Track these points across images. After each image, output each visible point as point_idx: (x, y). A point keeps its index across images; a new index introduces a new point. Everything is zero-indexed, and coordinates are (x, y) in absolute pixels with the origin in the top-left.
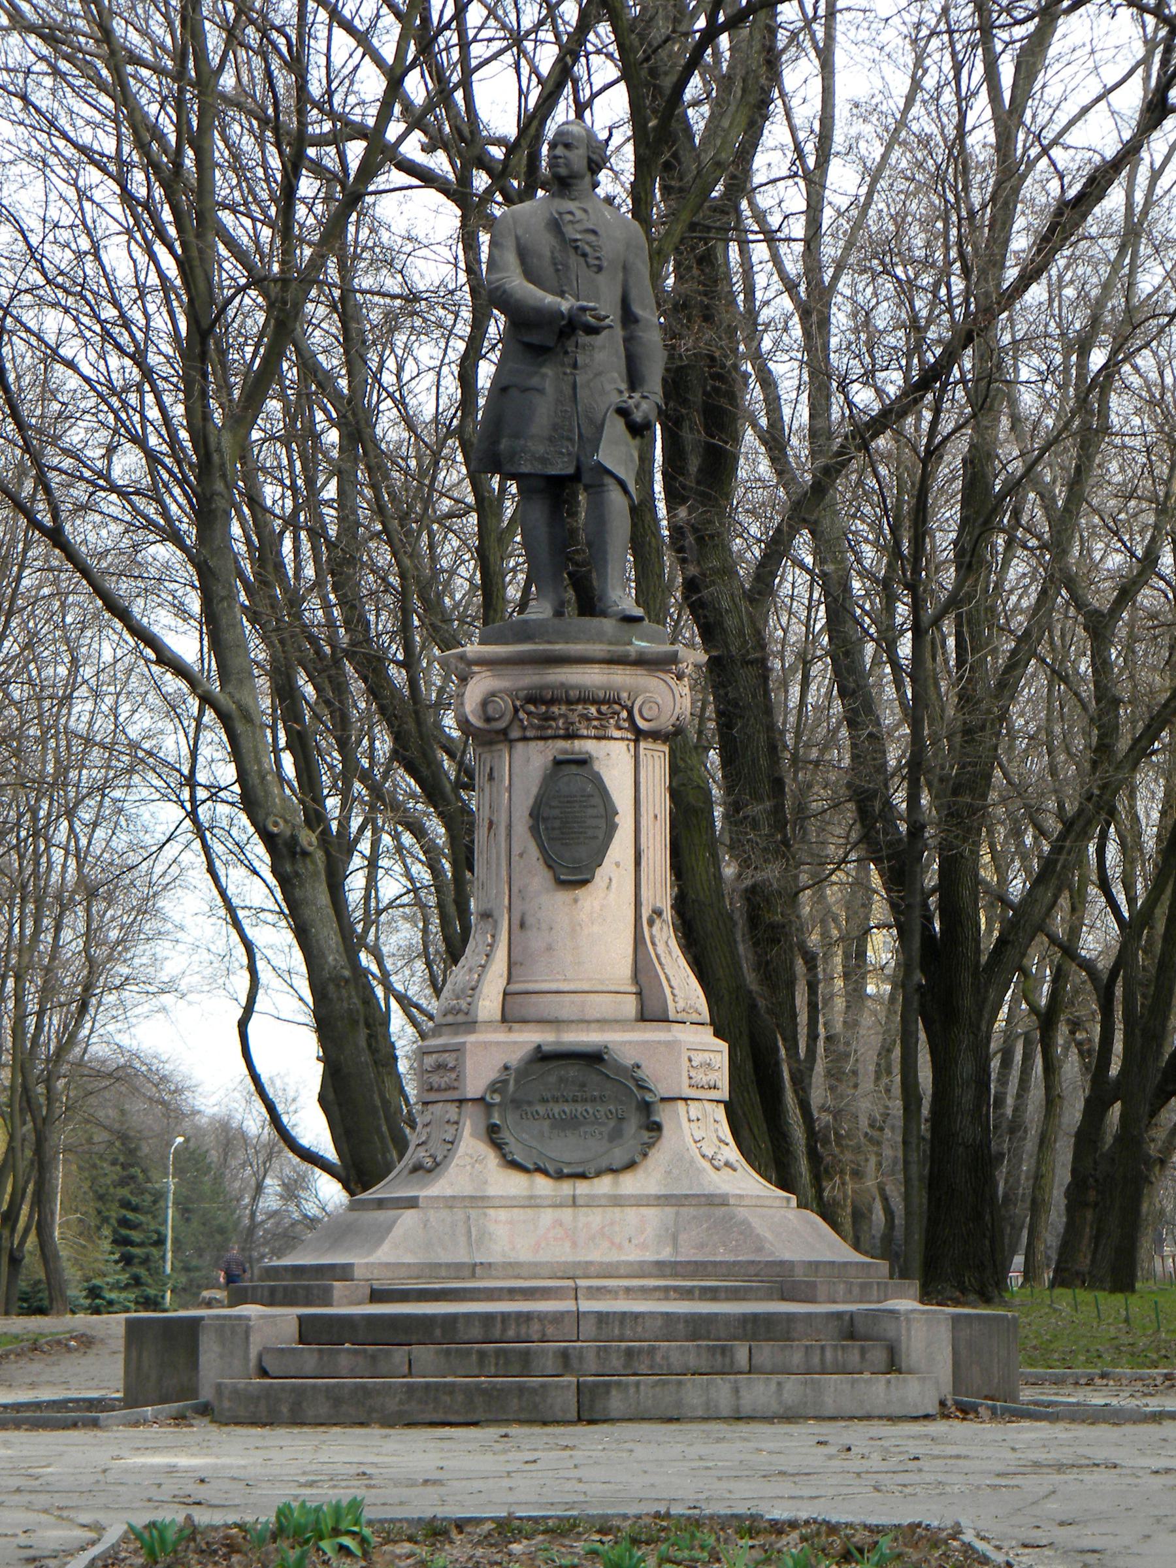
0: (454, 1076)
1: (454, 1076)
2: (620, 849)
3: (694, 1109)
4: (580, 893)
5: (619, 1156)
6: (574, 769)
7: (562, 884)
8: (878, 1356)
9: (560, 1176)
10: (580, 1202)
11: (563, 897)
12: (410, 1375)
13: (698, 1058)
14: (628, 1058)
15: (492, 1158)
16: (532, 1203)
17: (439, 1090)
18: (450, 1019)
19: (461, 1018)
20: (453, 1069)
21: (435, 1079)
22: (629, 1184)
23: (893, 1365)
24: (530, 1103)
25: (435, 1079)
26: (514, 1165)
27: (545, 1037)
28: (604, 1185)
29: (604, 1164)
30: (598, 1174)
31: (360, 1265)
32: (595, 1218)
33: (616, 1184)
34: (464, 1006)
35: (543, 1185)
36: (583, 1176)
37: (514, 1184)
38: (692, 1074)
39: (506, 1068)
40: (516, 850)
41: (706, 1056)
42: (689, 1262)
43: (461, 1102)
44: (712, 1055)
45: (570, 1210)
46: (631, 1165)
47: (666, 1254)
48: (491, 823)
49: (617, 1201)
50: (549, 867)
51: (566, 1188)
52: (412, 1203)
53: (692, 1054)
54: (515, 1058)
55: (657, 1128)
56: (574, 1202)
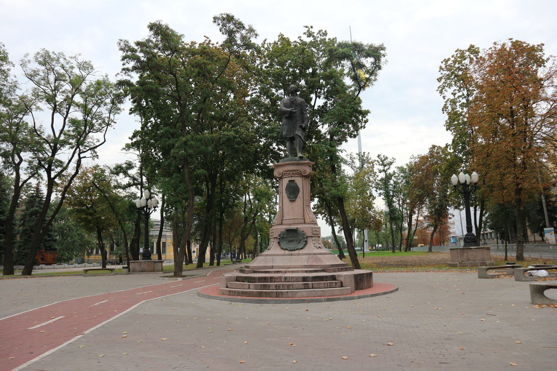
2: (300, 195)
5: (300, 247)
8: (340, 284)
9: (291, 250)
12: (249, 289)
13: (314, 229)
14: (302, 230)
15: (279, 248)
16: (284, 255)
22: (301, 252)
23: (342, 286)
26: (282, 248)
27: (288, 227)
28: (297, 252)
32: (294, 257)
35: (287, 252)
37: (283, 252)
46: (302, 248)
47: (306, 264)
49: (299, 254)
51: (291, 252)
54: (283, 230)
55: (306, 242)
56: (292, 255)
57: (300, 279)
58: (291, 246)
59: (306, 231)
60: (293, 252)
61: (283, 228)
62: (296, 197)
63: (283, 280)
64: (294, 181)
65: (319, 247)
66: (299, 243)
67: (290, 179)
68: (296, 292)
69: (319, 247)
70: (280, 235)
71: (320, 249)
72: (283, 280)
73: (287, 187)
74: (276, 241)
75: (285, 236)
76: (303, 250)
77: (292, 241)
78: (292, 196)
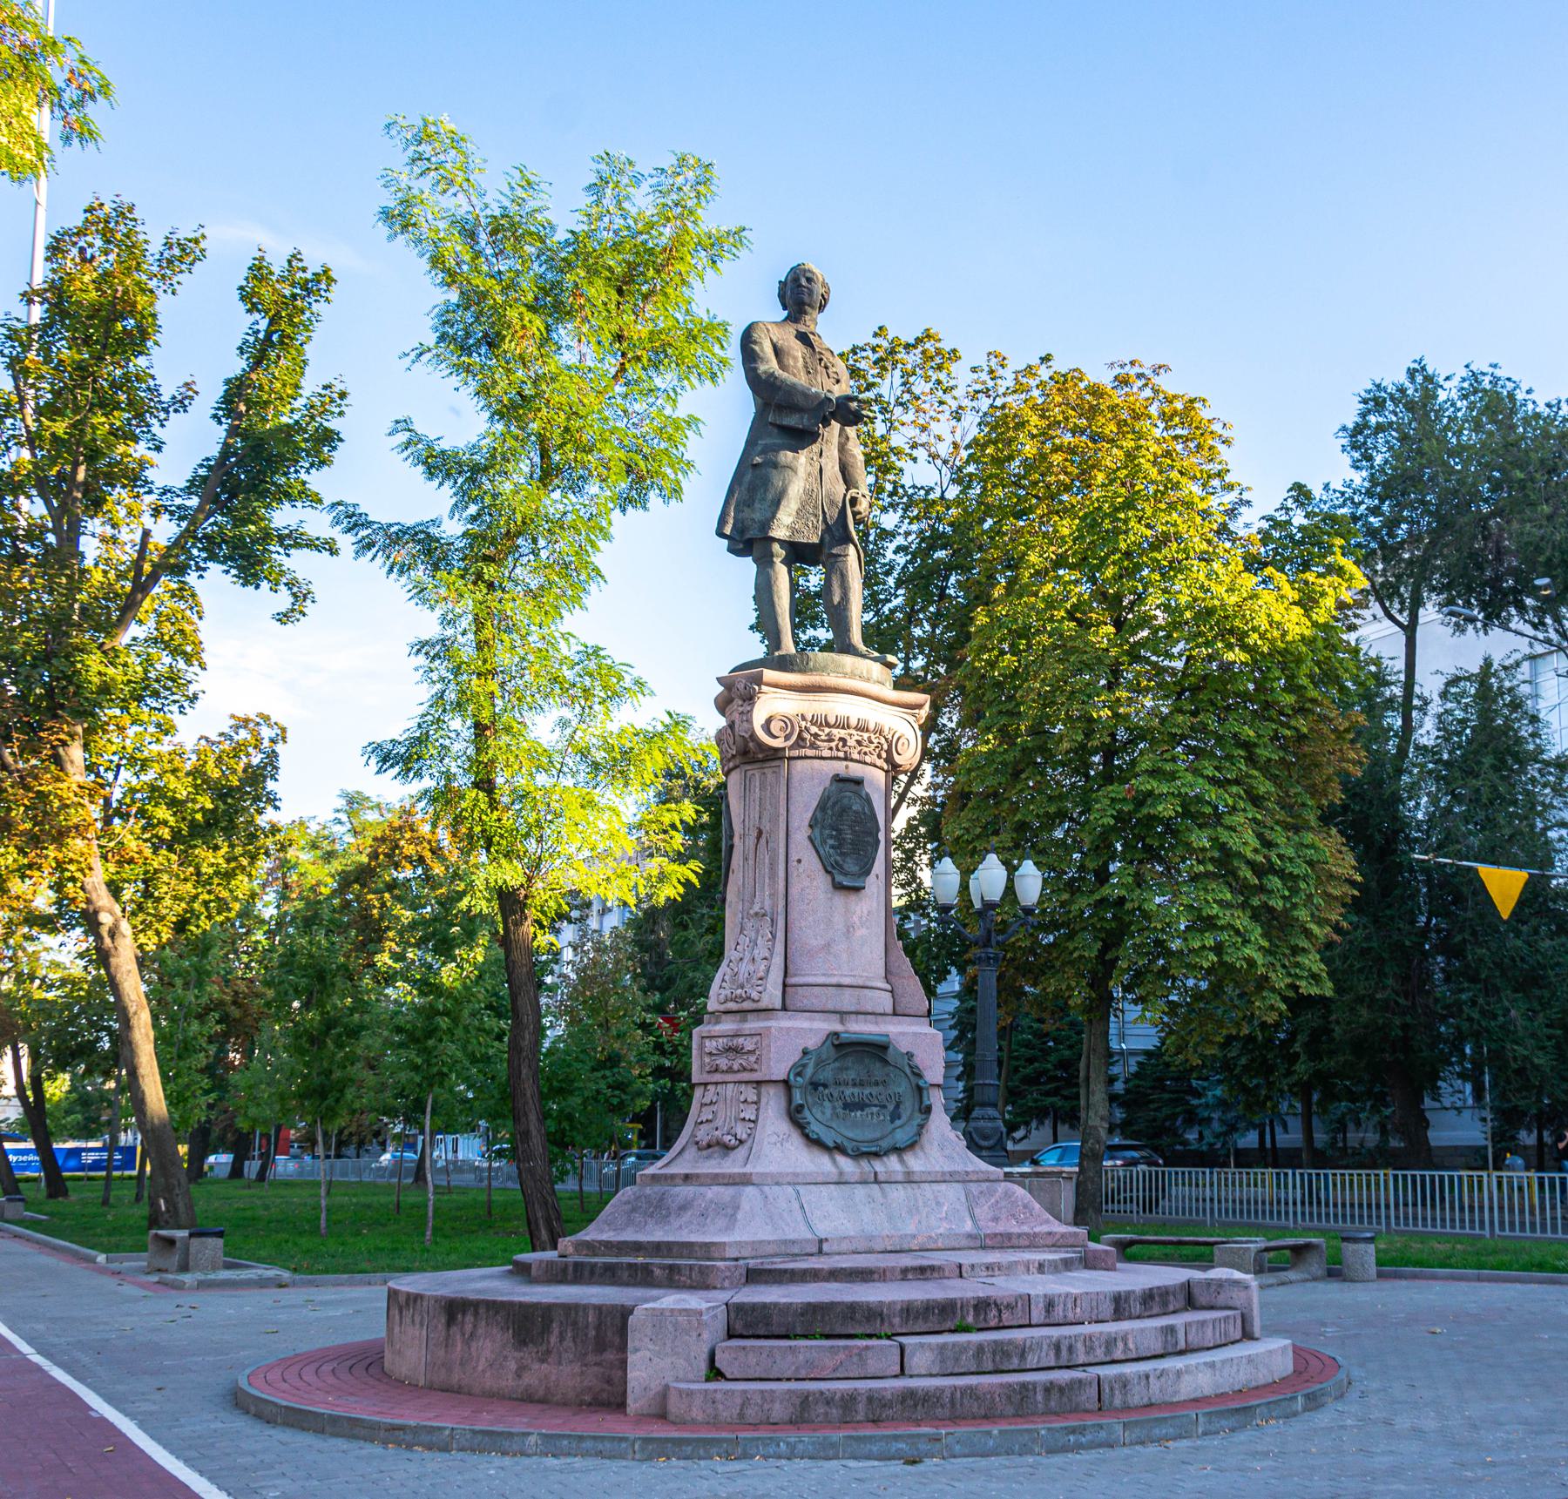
0: (753, 1059)
1: (753, 1059)
4: (853, 897)
5: (901, 1137)
6: (852, 787)
7: (838, 887)
9: (858, 1155)
10: (881, 1177)
11: (839, 899)
15: (796, 1139)
17: (730, 1070)
18: (732, 1006)
19: (747, 1005)
20: (751, 1052)
21: (723, 1062)
22: (915, 1162)
24: (825, 1086)
25: (723, 1062)
26: (815, 1142)
27: (838, 1027)
28: (893, 1162)
30: (886, 1154)
31: (731, 1244)
32: (898, 1194)
34: (755, 995)
36: (876, 1155)
39: (805, 1052)
40: (794, 857)
42: (996, 1235)
43: (759, 1083)
46: (911, 1146)
48: (760, 833)
49: (909, 1179)
50: (827, 871)
52: (744, 1180)
54: (812, 1042)
57: (1107, 1309)
58: (863, 1128)
59: (921, 1059)
60: (878, 1166)
61: (811, 1031)
62: (868, 873)
63: (1037, 1315)
64: (859, 782)
67: (839, 767)
68: (1179, 1373)
70: (798, 1069)
72: (1037, 1315)
73: (822, 807)
74: (773, 1103)
75: (826, 1075)
77: (861, 1106)
78: (850, 866)
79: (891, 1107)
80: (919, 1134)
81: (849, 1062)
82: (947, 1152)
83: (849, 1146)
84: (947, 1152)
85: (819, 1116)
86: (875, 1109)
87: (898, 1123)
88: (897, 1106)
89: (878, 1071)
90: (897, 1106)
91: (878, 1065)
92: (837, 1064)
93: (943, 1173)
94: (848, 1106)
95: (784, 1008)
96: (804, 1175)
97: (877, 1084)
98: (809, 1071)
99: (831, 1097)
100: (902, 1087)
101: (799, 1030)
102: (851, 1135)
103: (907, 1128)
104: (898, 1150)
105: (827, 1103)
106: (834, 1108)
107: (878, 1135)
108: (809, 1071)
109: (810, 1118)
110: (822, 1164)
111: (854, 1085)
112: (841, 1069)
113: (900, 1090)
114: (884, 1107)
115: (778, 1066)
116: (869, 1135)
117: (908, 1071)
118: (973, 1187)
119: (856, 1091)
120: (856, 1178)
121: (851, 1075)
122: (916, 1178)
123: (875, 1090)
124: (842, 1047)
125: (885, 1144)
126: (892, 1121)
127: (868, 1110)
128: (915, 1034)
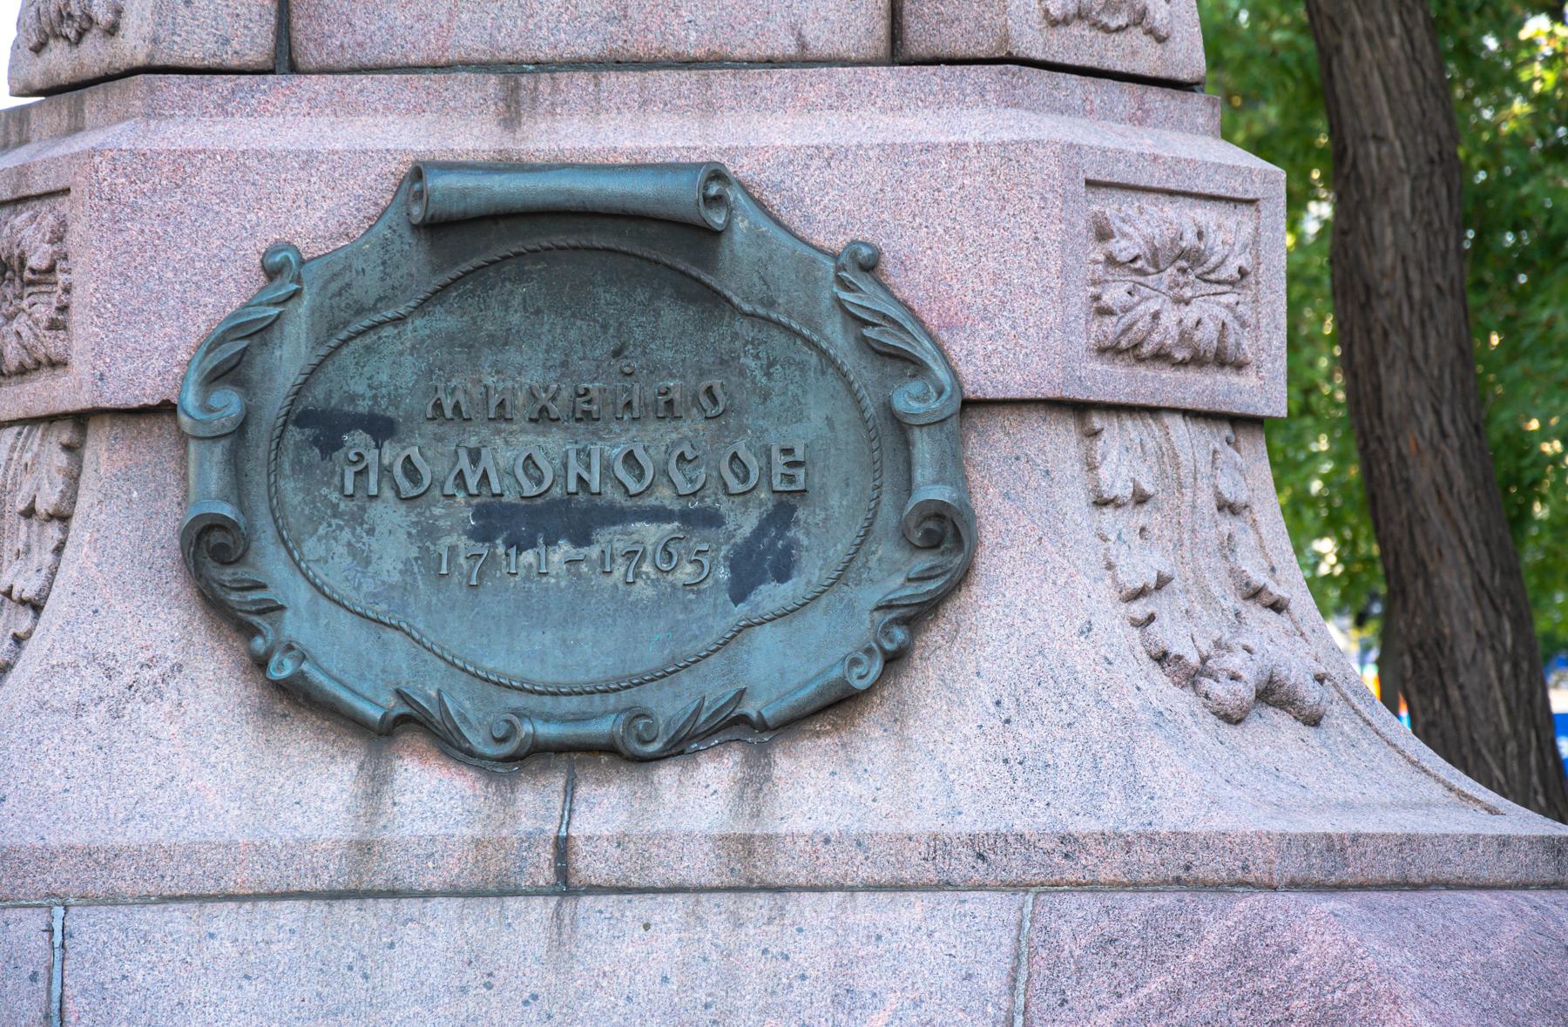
3: (1123, 456)
10: (588, 866)
13: (1143, 225)
15: (213, 683)
16: (363, 884)
22: (820, 793)
24: (382, 428)
26: (297, 699)
27: (458, 133)
28: (698, 799)
29: (708, 689)
30: (683, 745)
33: (755, 783)
35: (432, 799)
38: (1115, 295)
39: (277, 268)
41: (1186, 219)
44: (1206, 215)
45: (542, 908)
46: (836, 706)
49: (750, 874)
51: (535, 804)
53: (1110, 207)
58: (556, 633)
60: (603, 811)
65: (1271, 694)
66: (759, 563)
69: (1271, 694)
70: (233, 358)
71: (1276, 734)
74: (126, 515)
76: (872, 739)
77: (575, 518)
79: (744, 523)
80: (895, 660)
81: (508, 308)
82: (1029, 736)
83: (461, 703)
84: (1029, 736)
85: (335, 574)
86: (651, 534)
87: (772, 595)
88: (783, 512)
89: (668, 339)
90: (783, 512)
91: (671, 314)
92: (445, 320)
93: (938, 846)
94: (508, 523)
95: (284, 60)
96: (143, 856)
97: (669, 410)
98: (288, 359)
99: (413, 489)
100: (813, 422)
101: (236, 163)
102: (496, 662)
103: (817, 622)
104: (748, 731)
105: (389, 516)
106: (427, 532)
107: (651, 656)
108: (288, 359)
109: (294, 593)
110: (314, 794)
111: (542, 418)
112: (468, 345)
113: (799, 437)
114: (712, 519)
115: (136, 331)
116: (593, 653)
117: (836, 335)
118: (1076, 917)
119: (551, 446)
120: (452, 869)
121: (527, 370)
122: (786, 868)
123: (653, 441)
124: (471, 239)
125: (670, 706)
126: (739, 596)
127: (611, 539)
128: (894, 152)
